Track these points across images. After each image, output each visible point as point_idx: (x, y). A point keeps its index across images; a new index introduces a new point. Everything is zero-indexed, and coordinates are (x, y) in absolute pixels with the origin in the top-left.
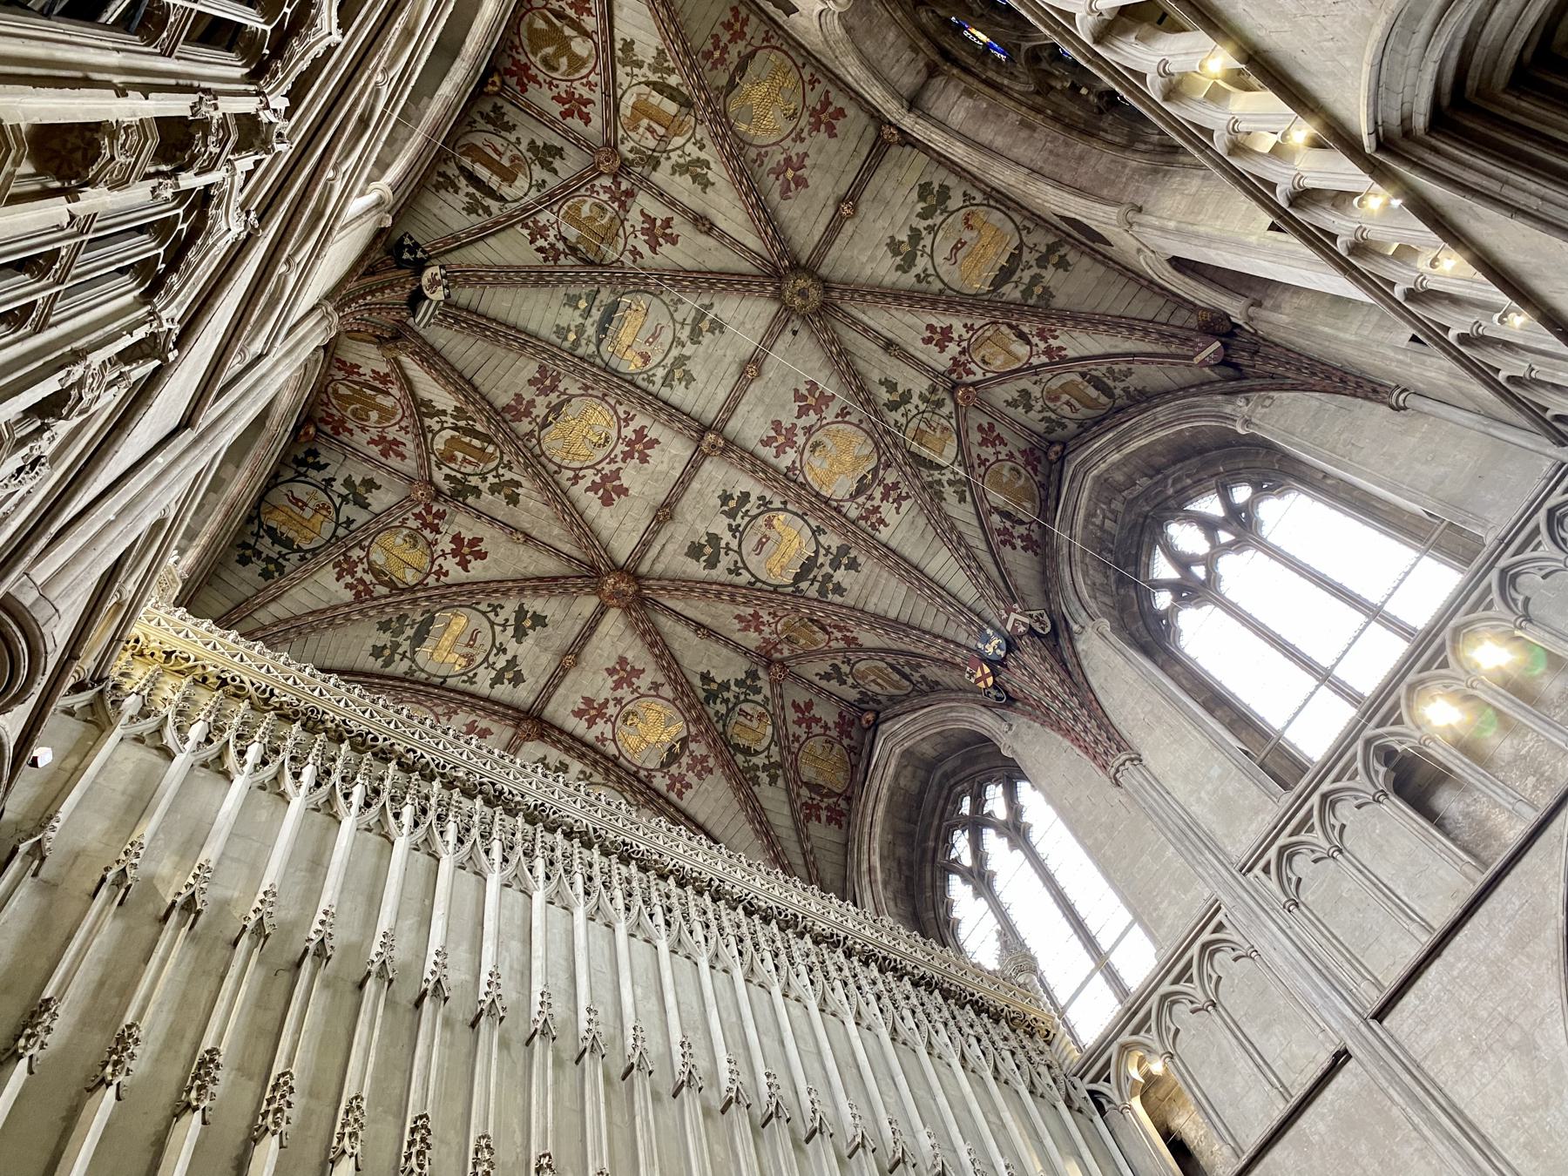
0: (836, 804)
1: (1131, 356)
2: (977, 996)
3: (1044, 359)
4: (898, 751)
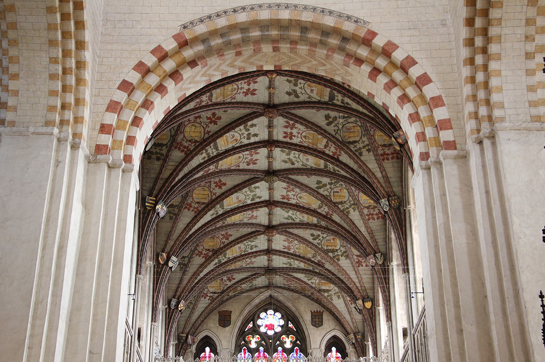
1: (192, 313)
3: (205, 292)
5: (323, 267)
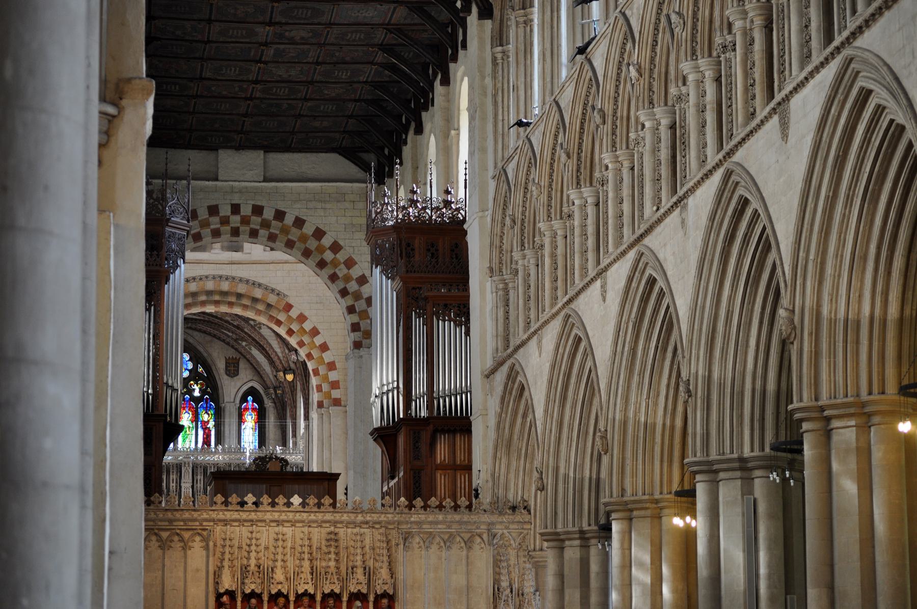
5: (243, 331)
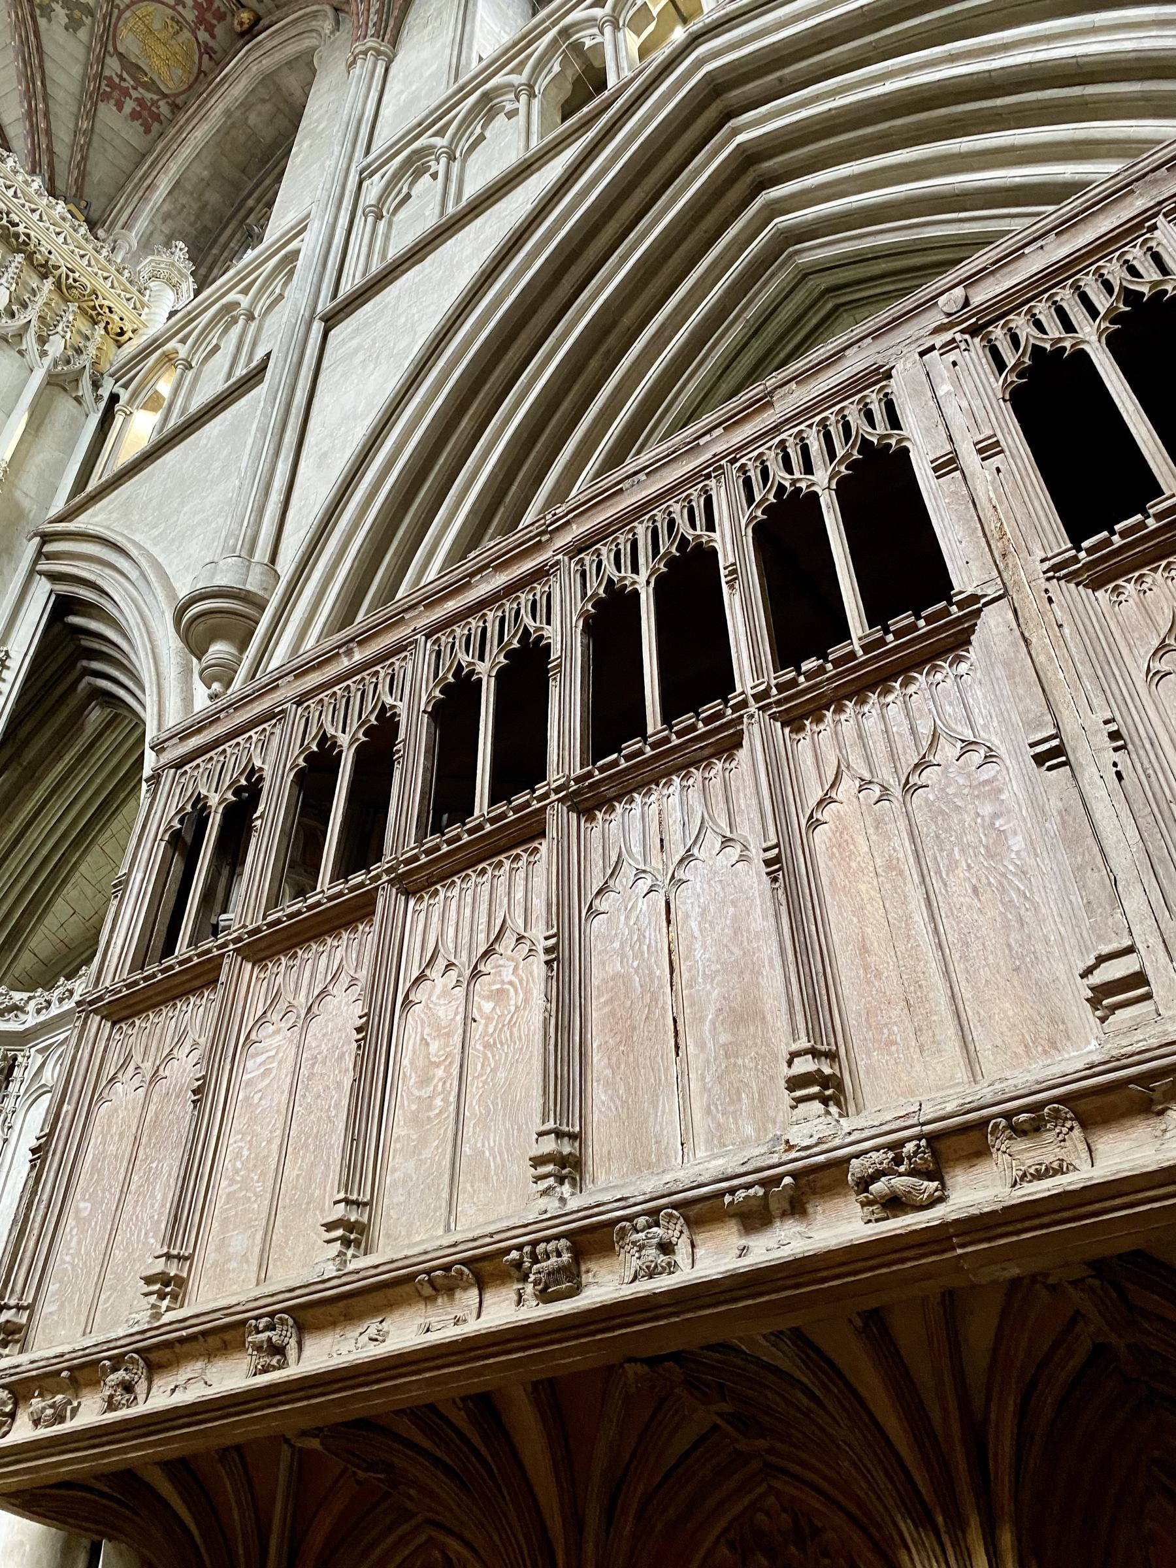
0: (154, 103)
2: (21, 229)
4: (255, 68)
